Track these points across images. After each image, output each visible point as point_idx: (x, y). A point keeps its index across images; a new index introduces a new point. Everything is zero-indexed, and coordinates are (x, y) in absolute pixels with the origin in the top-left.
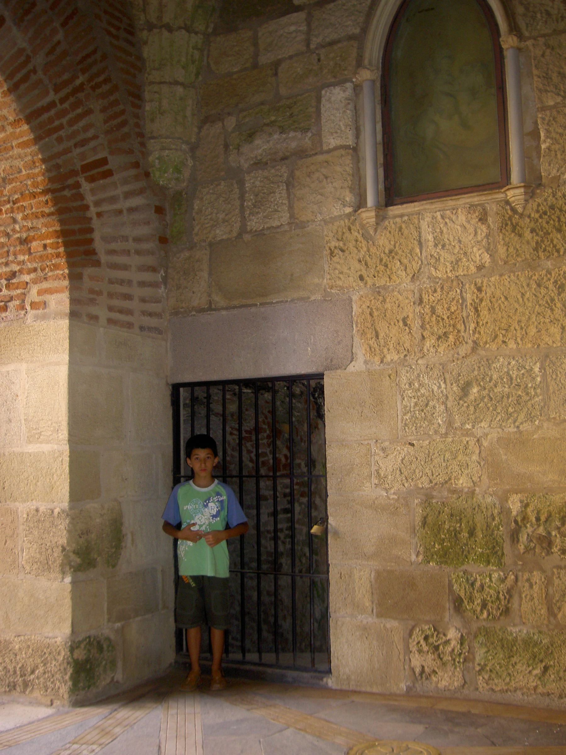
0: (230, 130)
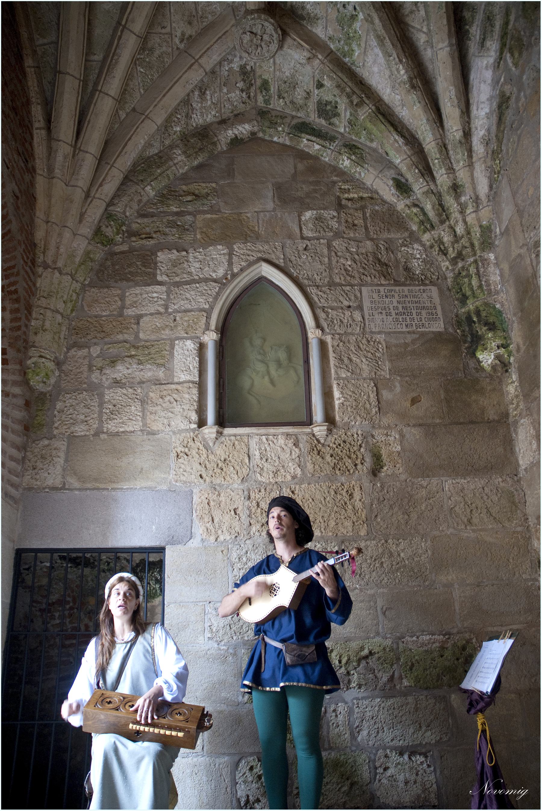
0: (95, 355)
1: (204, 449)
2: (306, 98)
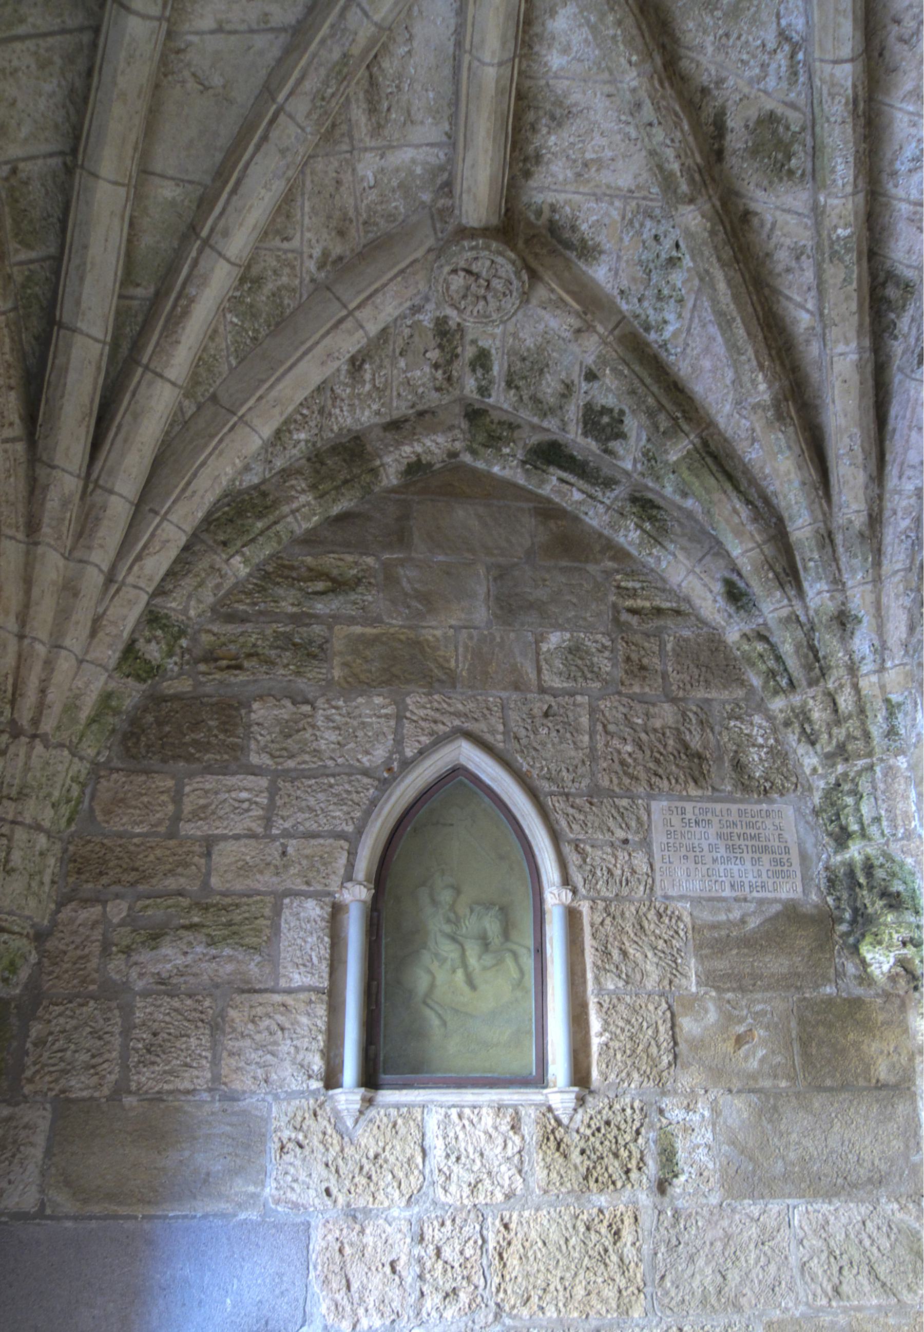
0: (115, 921)
1: (334, 1135)
2: (563, 396)
